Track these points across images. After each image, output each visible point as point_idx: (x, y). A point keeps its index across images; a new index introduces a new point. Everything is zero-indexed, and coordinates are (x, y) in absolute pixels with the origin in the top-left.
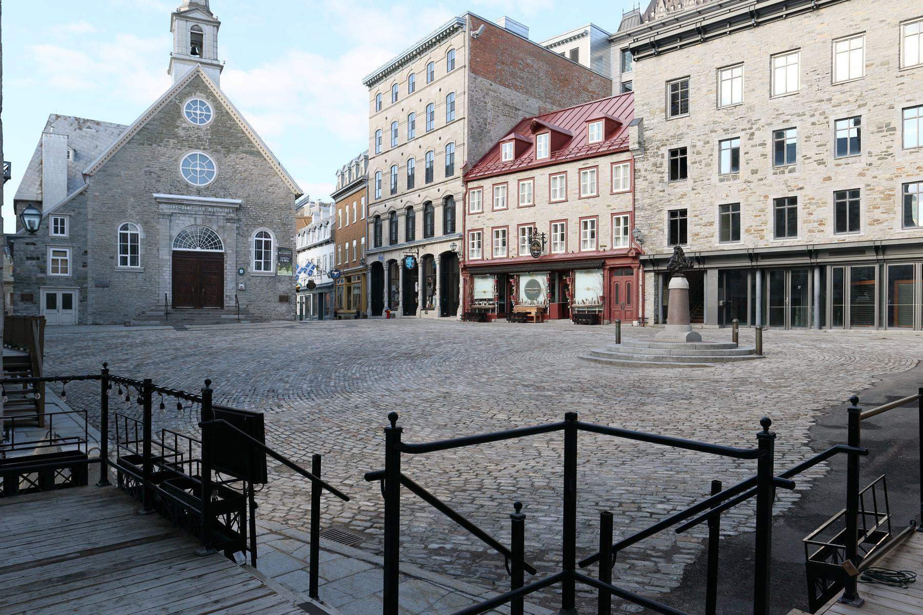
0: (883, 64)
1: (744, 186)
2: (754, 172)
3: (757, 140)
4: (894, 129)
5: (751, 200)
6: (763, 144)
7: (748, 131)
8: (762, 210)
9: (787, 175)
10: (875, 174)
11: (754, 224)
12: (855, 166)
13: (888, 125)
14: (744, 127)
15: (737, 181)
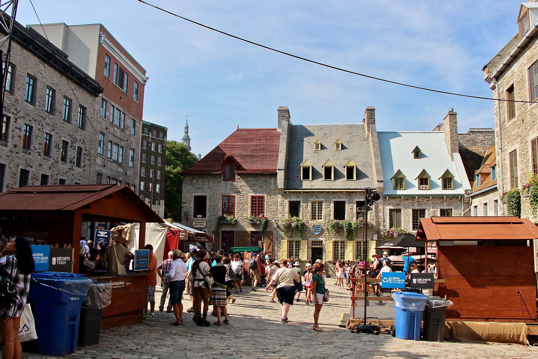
0: (60, 113)
1: (9, 154)
2: (15, 146)
3: (18, 125)
4: (59, 149)
5: (12, 165)
6: (20, 129)
7: (15, 116)
8: (15, 174)
9: (27, 156)
10: (54, 169)
11: (10, 182)
12: (49, 162)
13: (58, 146)
14: (13, 111)
15: (6, 149)
